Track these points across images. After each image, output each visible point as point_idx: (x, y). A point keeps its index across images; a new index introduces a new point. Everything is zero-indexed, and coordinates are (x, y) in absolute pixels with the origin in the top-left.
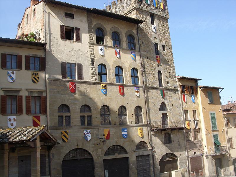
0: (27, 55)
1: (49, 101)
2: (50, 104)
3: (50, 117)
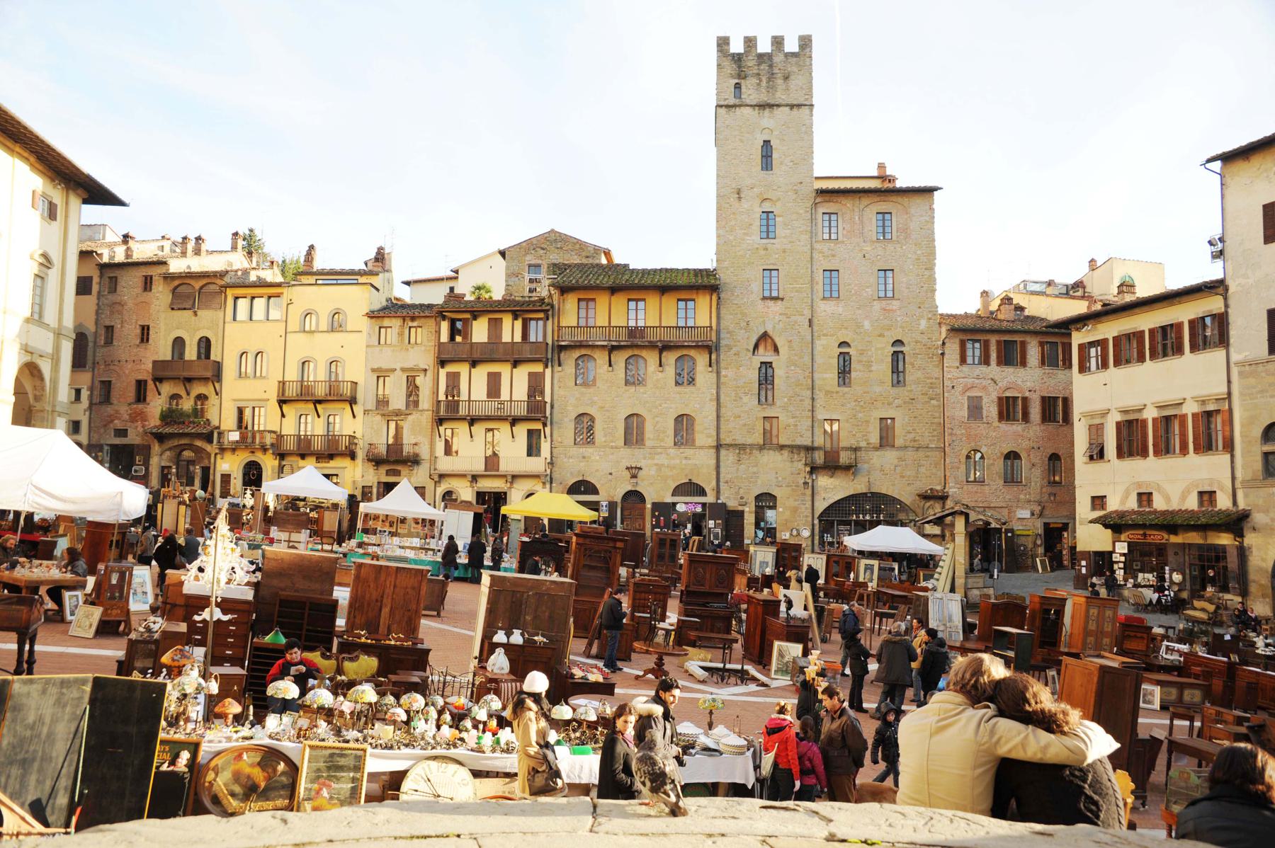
0: (1192, 317)
1: (1241, 417)
2: (1242, 426)
3: (1242, 456)
